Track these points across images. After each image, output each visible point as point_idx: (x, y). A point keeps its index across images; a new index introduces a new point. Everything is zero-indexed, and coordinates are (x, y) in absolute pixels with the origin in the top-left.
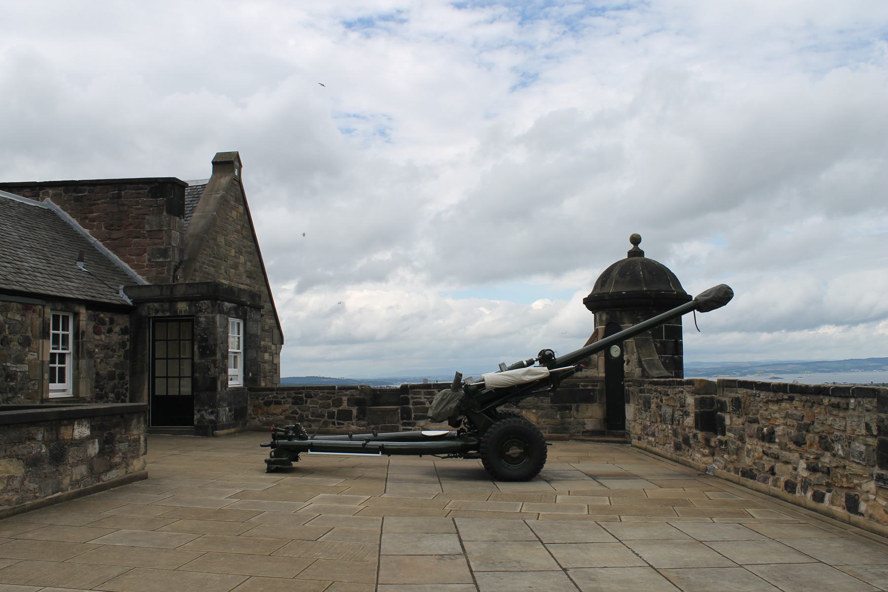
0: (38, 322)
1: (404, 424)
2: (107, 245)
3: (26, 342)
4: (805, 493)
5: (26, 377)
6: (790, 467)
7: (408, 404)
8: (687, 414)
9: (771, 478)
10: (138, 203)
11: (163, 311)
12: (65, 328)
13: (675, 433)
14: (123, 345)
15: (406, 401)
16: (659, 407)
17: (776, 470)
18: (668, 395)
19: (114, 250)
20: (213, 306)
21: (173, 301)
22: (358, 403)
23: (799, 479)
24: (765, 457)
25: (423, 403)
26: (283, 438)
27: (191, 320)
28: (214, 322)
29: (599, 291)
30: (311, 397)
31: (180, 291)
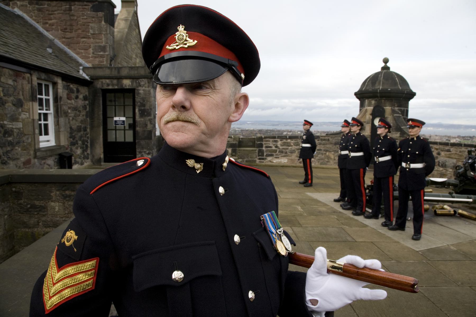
0: (27, 87)
1: (260, 159)
2: (63, 43)
3: (19, 104)
5: (21, 133)
7: (262, 147)
10: (83, 15)
11: (113, 85)
12: (47, 94)
14: (85, 107)
15: (261, 146)
19: (68, 45)
20: (149, 83)
21: (120, 78)
27: (132, 92)
28: (150, 93)
31: (125, 72)
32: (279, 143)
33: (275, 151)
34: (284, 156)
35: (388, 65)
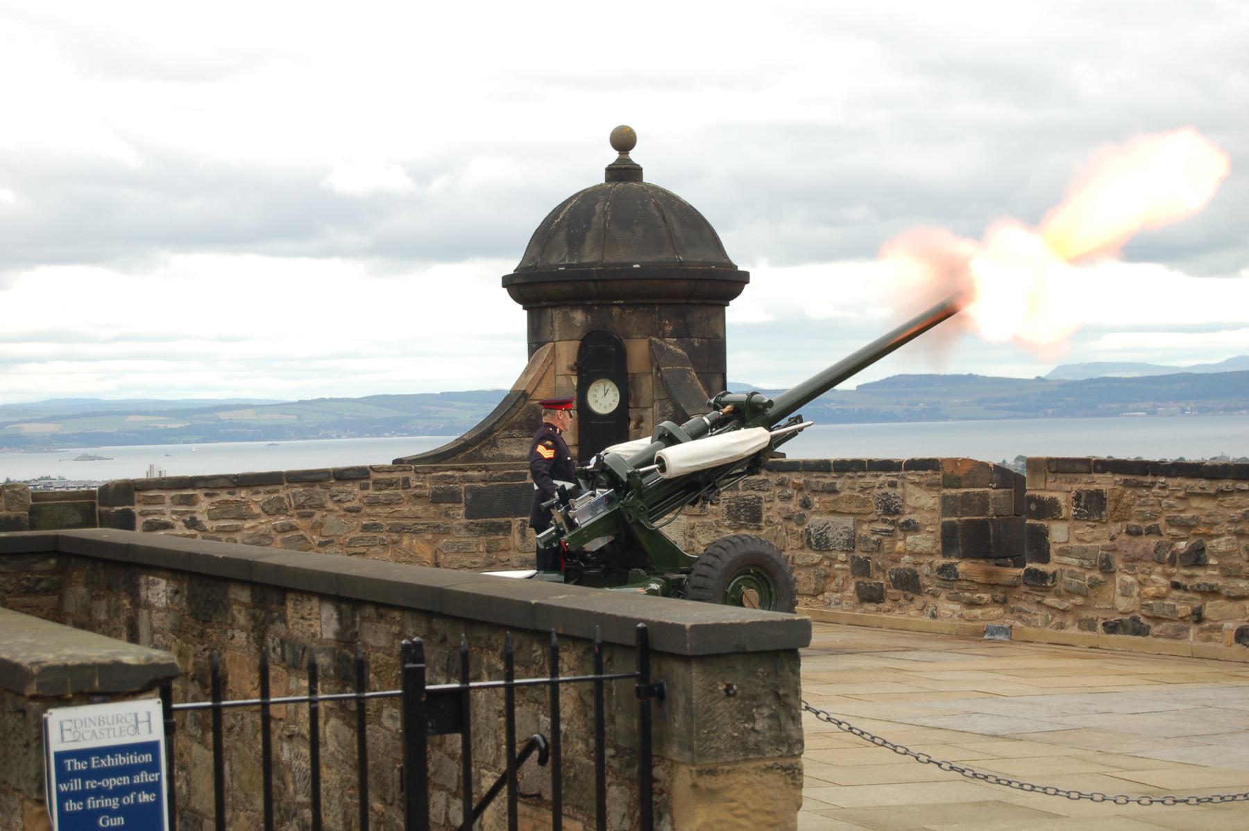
8: (910, 528)
25: (167, 526)
29: (560, 259)
32: (203, 505)
35: (635, 155)
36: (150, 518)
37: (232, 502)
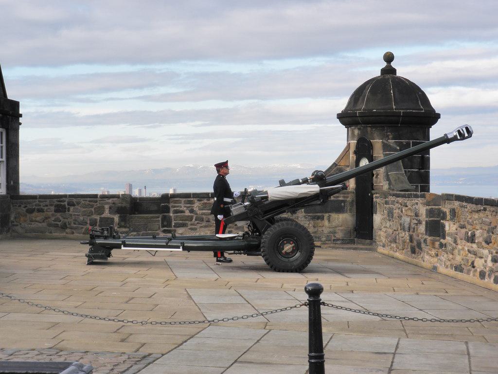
1: (164, 231)
4: (490, 278)
6: (483, 260)
7: (169, 212)
8: (420, 222)
9: (473, 269)
13: (411, 240)
15: (167, 210)
16: (400, 217)
17: (475, 264)
18: (407, 206)
22: (120, 211)
23: (487, 269)
24: (469, 255)
25: (183, 212)
26: (98, 237)
30: (74, 205)
32: (197, 205)
33: (191, 218)
34: (206, 227)
35: (393, 64)
36: (175, 209)
37: (208, 204)
